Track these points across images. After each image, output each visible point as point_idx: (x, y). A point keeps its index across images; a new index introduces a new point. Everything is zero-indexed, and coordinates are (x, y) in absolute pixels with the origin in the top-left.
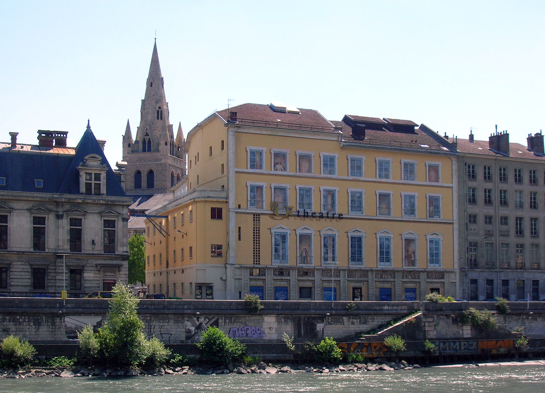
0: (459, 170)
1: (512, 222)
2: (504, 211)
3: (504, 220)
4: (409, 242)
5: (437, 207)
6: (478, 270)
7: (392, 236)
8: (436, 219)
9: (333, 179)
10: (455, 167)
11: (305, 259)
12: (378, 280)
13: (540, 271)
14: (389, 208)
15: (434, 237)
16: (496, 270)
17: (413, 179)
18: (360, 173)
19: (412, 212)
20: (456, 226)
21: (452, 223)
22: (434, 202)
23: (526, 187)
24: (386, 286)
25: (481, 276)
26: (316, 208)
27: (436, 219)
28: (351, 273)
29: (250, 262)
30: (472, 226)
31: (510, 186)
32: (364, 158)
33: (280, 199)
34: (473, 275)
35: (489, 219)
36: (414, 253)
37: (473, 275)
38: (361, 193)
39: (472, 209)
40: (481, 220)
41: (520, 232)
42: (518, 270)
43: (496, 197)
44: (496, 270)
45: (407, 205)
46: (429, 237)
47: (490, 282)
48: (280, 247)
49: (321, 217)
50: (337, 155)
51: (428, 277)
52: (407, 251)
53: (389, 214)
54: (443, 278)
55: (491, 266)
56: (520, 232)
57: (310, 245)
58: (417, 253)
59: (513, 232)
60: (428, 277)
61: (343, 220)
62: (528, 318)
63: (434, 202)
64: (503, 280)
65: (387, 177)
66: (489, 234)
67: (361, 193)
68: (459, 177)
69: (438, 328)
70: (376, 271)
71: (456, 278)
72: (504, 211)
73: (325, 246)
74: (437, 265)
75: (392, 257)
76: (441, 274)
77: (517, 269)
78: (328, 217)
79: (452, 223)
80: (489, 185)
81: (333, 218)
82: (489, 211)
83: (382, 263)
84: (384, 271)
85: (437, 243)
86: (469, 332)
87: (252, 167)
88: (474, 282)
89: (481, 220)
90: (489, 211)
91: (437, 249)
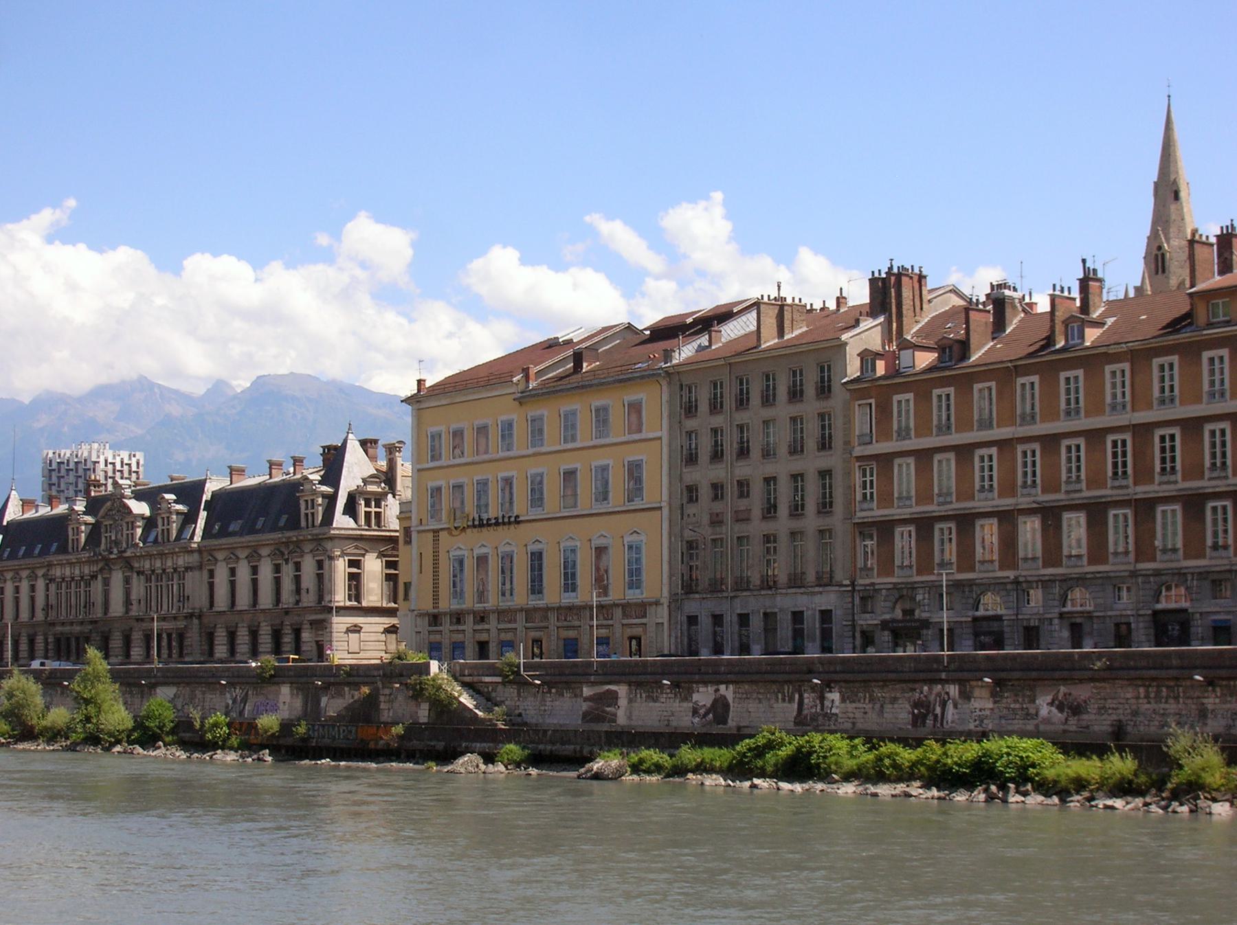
0: (670, 402)
1: (757, 488)
2: (743, 470)
3: (743, 487)
4: (600, 551)
5: (639, 480)
6: (697, 596)
7: (578, 544)
8: (638, 504)
9: (511, 458)
10: (665, 397)
11: (481, 595)
12: (560, 624)
13: (802, 590)
14: (575, 495)
15: (635, 537)
16: (725, 594)
17: (607, 436)
18: (542, 440)
19: (604, 496)
20: (666, 511)
21: (660, 508)
22: (634, 472)
23: (783, 410)
24: (572, 634)
25: (700, 607)
26: (493, 512)
27: (638, 504)
28: (529, 613)
29: (428, 606)
30: (691, 509)
31: (754, 415)
32: (546, 413)
33: (458, 504)
34: (691, 607)
35: (717, 490)
36: (606, 571)
37: (691, 607)
38: (542, 475)
39: (694, 475)
40: (705, 493)
41: (770, 510)
42: (763, 592)
43: (730, 445)
44: (725, 594)
45: (599, 485)
46: (627, 539)
47: (717, 619)
48: (458, 580)
49: (497, 524)
50: (515, 417)
51: (625, 615)
52: (598, 569)
53: (575, 506)
54: (644, 616)
55: (716, 587)
56: (770, 510)
57: (487, 572)
58: (610, 572)
59: (757, 512)
60: (625, 615)
61: (522, 525)
62: (550, 692)
63: (634, 472)
64: (740, 615)
65: (574, 439)
66: (716, 521)
67: (542, 475)
68: (671, 416)
69: (396, 705)
70: (559, 608)
71: (662, 614)
72: (743, 470)
73: (503, 572)
74: (638, 591)
75: (579, 582)
76: (642, 608)
77: (762, 589)
78: (504, 523)
79: (660, 508)
80: (718, 421)
81: (510, 523)
82: (718, 472)
83: (567, 594)
84: (570, 608)
85: (638, 549)
86: (426, 713)
87: (433, 458)
88: (692, 620)
89: (705, 493)
90: (718, 472)
91: (638, 560)
